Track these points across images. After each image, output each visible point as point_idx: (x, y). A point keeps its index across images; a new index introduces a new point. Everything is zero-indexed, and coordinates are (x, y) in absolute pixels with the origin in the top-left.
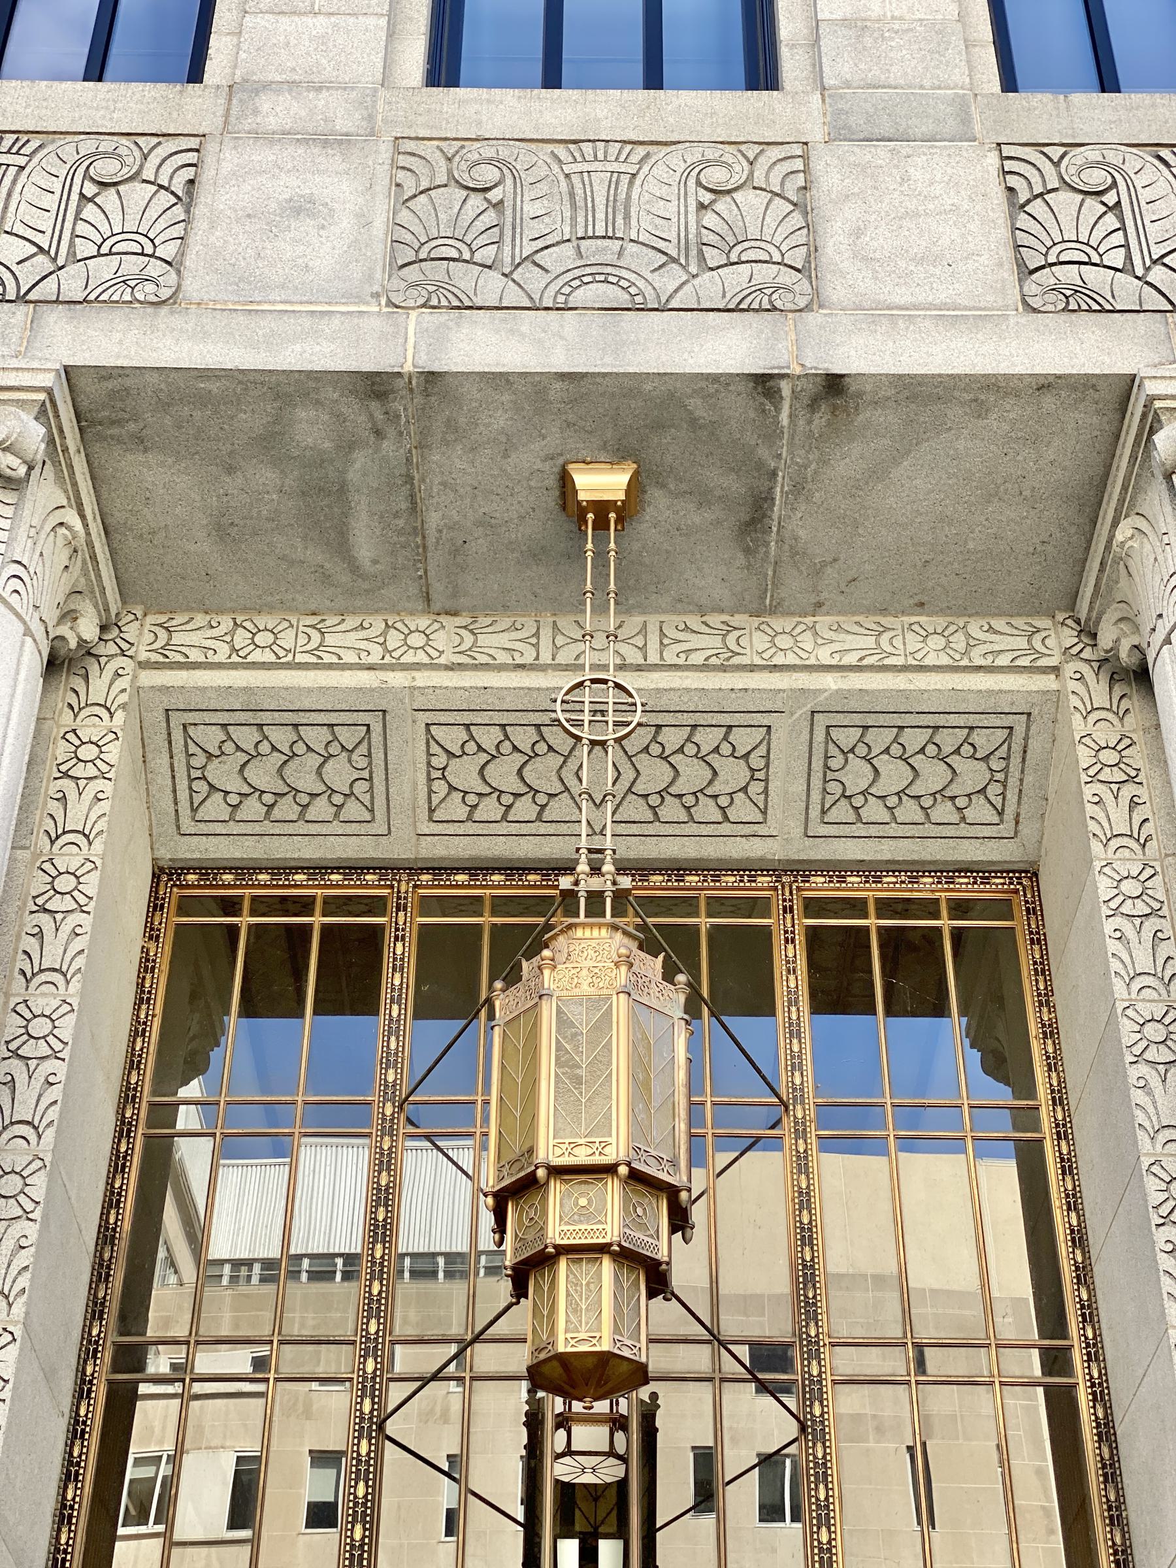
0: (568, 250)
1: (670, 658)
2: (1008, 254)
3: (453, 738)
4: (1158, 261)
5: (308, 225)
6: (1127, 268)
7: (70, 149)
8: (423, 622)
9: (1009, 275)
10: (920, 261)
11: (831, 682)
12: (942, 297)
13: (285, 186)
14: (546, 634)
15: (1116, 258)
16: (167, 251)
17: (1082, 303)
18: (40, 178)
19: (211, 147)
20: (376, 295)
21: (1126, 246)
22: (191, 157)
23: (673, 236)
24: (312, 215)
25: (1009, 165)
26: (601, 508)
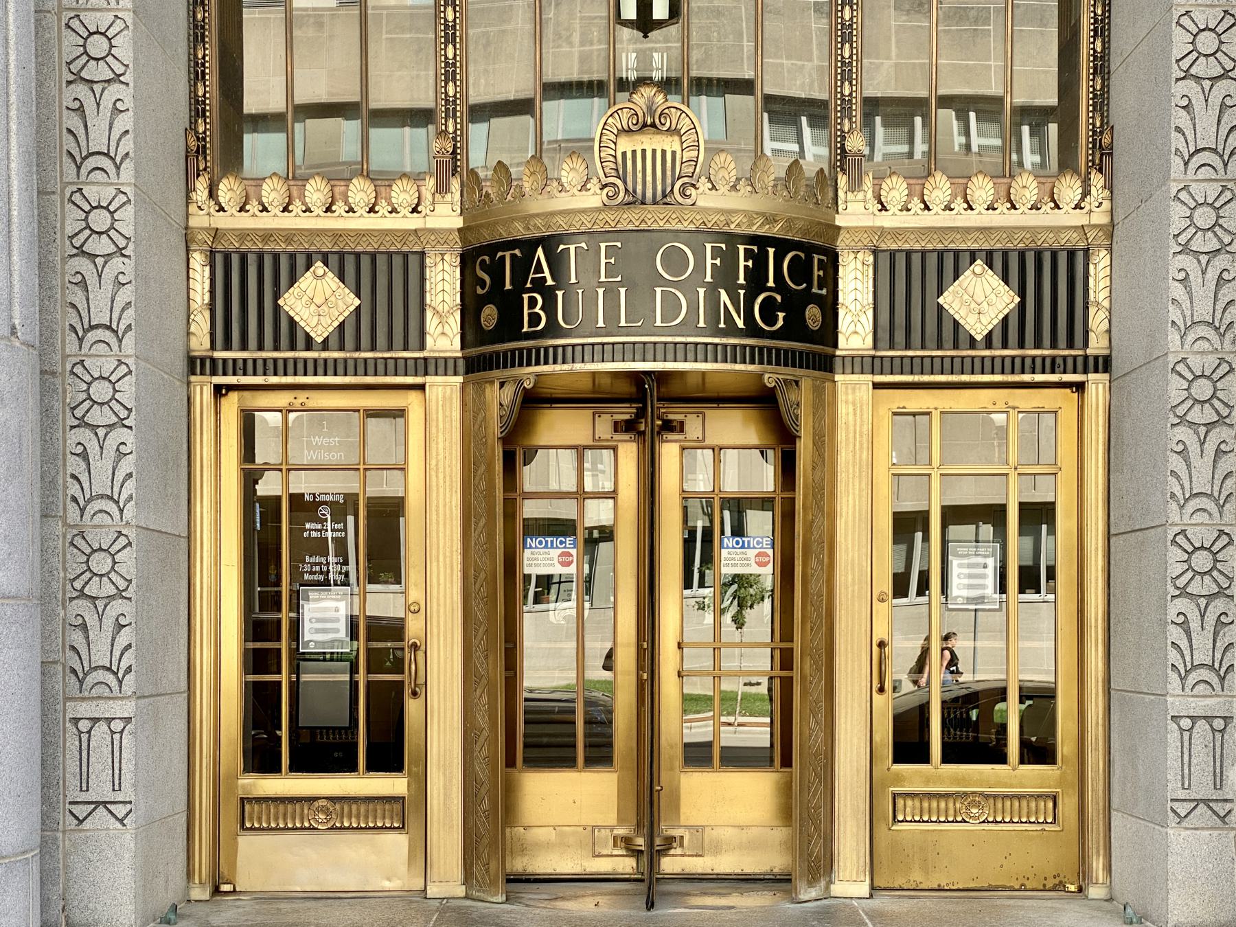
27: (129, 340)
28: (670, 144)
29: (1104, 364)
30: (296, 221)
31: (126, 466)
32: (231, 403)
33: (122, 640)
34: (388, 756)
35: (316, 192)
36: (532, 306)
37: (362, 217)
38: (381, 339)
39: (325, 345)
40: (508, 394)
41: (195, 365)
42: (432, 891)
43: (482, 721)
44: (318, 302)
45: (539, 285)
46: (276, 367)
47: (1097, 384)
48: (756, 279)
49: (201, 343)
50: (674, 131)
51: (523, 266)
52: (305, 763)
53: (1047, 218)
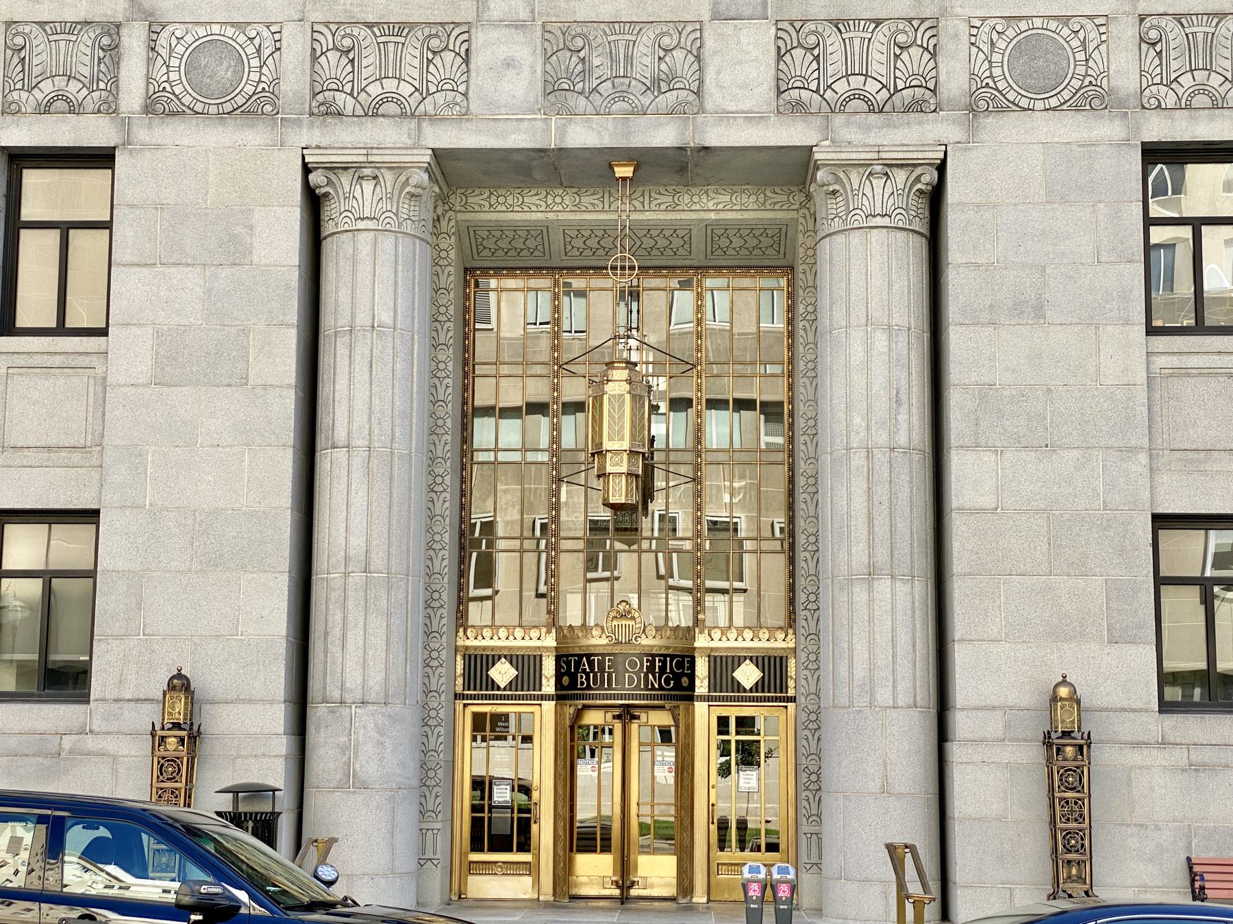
0: (609, 84)
1: (653, 207)
2: (773, 84)
4: (829, 87)
5: (511, 73)
6: (817, 91)
7: (420, 33)
9: (773, 94)
11: (712, 216)
12: (746, 107)
13: (503, 52)
14: (606, 195)
15: (813, 86)
16: (462, 88)
17: (798, 108)
18: (411, 50)
19: (473, 31)
20: (539, 110)
21: (818, 79)
22: (465, 36)
23: (648, 76)
24: (514, 68)
25: (781, 34)
27: (443, 696)
28: (632, 623)
31: (441, 739)
33: (438, 801)
34: (524, 847)
36: (582, 678)
38: (526, 687)
39: (505, 689)
40: (572, 710)
42: (542, 898)
43: (561, 833)
45: (584, 671)
48: (663, 669)
50: (633, 618)
51: (578, 664)
52: (492, 849)
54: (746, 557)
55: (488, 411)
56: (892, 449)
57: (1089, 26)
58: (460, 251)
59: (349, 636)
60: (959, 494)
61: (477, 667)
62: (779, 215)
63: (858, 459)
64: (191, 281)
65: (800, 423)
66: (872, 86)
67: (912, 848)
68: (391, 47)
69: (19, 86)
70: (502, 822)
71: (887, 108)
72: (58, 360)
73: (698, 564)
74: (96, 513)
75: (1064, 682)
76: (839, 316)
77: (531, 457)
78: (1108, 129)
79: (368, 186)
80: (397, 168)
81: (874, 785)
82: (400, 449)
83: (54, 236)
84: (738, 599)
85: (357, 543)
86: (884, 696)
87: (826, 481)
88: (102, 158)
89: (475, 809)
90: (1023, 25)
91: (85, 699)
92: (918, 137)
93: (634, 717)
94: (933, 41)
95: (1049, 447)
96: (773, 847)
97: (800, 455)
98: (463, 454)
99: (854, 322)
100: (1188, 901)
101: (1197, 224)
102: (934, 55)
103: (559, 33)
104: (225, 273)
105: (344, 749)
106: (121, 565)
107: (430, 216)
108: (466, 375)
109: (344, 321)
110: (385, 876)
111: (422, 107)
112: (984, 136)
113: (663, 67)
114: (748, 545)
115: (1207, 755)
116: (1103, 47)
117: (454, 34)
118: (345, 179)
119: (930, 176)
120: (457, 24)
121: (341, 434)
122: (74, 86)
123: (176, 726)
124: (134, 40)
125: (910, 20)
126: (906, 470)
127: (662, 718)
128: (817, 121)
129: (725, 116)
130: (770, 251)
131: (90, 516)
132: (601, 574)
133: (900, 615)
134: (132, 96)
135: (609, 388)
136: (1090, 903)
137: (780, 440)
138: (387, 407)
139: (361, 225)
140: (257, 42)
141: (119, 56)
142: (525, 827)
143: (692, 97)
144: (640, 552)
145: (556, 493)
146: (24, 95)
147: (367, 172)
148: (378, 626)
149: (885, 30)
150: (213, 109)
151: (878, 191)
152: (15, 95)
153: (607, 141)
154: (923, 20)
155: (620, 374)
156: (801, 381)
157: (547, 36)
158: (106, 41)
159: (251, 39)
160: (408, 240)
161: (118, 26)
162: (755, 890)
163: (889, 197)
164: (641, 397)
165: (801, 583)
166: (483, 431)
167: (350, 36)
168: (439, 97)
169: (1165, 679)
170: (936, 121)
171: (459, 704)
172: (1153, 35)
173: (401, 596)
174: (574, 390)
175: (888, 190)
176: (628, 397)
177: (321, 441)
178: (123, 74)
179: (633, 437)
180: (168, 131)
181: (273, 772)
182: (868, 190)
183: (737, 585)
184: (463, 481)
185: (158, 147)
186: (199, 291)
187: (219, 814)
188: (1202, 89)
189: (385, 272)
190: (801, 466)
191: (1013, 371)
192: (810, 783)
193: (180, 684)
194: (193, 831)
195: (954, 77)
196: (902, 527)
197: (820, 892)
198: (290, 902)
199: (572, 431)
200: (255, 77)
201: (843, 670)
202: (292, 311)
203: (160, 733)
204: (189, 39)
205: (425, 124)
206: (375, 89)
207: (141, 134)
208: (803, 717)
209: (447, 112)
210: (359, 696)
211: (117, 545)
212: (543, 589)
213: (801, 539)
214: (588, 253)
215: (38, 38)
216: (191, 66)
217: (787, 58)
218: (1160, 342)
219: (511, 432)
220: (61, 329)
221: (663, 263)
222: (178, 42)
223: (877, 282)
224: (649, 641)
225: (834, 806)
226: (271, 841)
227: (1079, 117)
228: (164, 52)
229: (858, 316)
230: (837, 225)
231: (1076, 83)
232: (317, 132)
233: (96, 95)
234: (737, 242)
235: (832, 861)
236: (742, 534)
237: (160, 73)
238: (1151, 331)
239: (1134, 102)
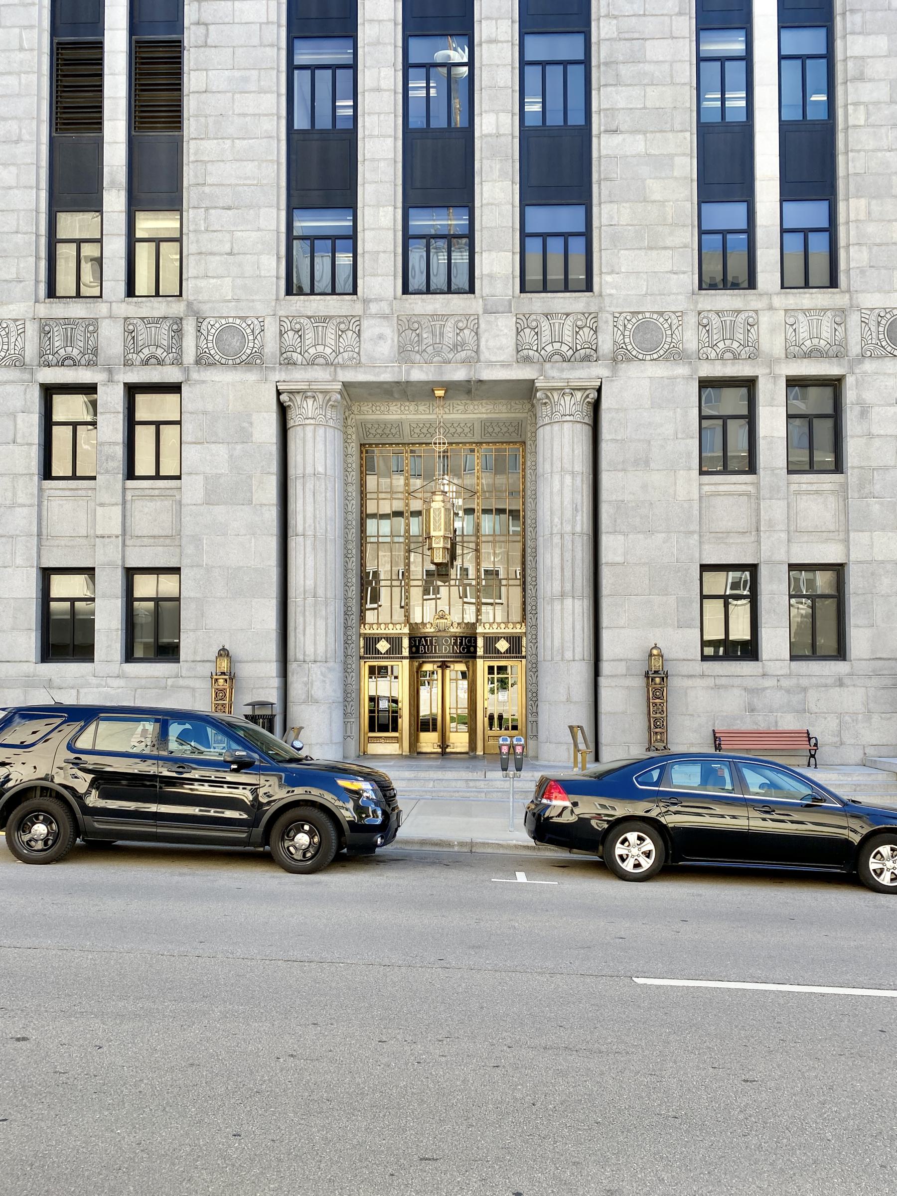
0: (431, 347)
2: (514, 347)
3: (415, 426)
5: (382, 342)
6: (537, 351)
8: (407, 404)
9: (515, 353)
10: (498, 349)
12: (502, 359)
13: (377, 331)
16: (357, 350)
17: (527, 360)
18: (330, 330)
22: (358, 323)
26: (440, 397)
29: (524, 657)
30: (379, 631)
32: (367, 664)
34: (395, 729)
35: (383, 626)
36: (421, 648)
37: (391, 631)
41: (361, 658)
44: (383, 646)
46: (375, 658)
47: (524, 660)
48: (461, 643)
49: (362, 654)
51: (420, 641)
52: (379, 731)
53: (514, 631)
54: (503, 588)
55: (373, 516)
56: (573, 534)
57: (673, 317)
58: (358, 434)
59: (307, 629)
60: (606, 556)
61: (371, 642)
62: (518, 415)
63: (557, 540)
64: (221, 451)
65: (528, 521)
66: (565, 348)
67: (581, 727)
68: (320, 328)
69: (132, 351)
70: (384, 718)
71: (572, 359)
72: (156, 492)
73: (478, 591)
74: (179, 569)
75: (656, 647)
76: (547, 467)
77: (396, 539)
78: (682, 370)
79: (310, 402)
80: (325, 392)
81: (564, 698)
82: (330, 536)
83: (153, 428)
84: (498, 607)
85: (310, 583)
86: (568, 655)
87: (540, 550)
88: (175, 388)
89: (371, 711)
90: (640, 316)
91: (177, 660)
92: (587, 374)
93: (447, 667)
94: (595, 325)
95: (651, 532)
96: (515, 728)
97: (528, 537)
98: (362, 538)
99: (555, 470)
100: (712, 751)
101: (725, 419)
102: (596, 332)
103: (405, 321)
104: (239, 447)
105: (306, 684)
106: (192, 595)
107: (342, 417)
108: (362, 499)
109: (300, 471)
110: (327, 744)
111: (336, 360)
112: (620, 373)
113: (459, 338)
114: (504, 582)
115: (723, 681)
116: (680, 328)
117: (352, 321)
118: (298, 398)
119: (593, 395)
120: (354, 316)
121: (300, 529)
122: (160, 351)
123: (223, 673)
124: (189, 327)
125: (583, 314)
126: (580, 544)
127: (462, 667)
128: (537, 366)
129: (491, 364)
130: (514, 434)
131: (176, 570)
132: (432, 596)
133: (576, 615)
134: (189, 356)
135: (433, 504)
136: (666, 752)
137: (518, 529)
138: (323, 515)
139: (307, 422)
140: (252, 326)
141: (182, 335)
142: (395, 720)
143: (473, 354)
144: (450, 586)
145: (408, 558)
146: (135, 356)
147: (309, 394)
148: (321, 624)
149: (571, 319)
150: (230, 362)
151: (568, 403)
152: (130, 356)
153: (431, 378)
154: (590, 314)
155: (438, 498)
156: (529, 500)
157: (400, 322)
158: (175, 327)
159: (249, 325)
160: (332, 430)
161: (181, 319)
162: (505, 750)
163: (573, 407)
164: (449, 509)
165: (528, 600)
166: (371, 525)
167: (299, 323)
168: (346, 355)
169: (704, 644)
170: (596, 366)
171: (362, 662)
172: (705, 321)
173: (332, 608)
174: (416, 505)
175: (572, 402)
176: (443, 510)
177: (290, 532)
178: (184, 344)
179: (446, 530)
180: (208, 373)
181: (273, 696)
182: (562, 402)
183: (498, 601)
184: (362, 552)
185: (203, 382)
186: (226, 456)
187: (246, 717)
188: (728, 350)
189: (320, 446)
190: (529, 543)
191: (634, 494)
192: (533, 698)
193: (224, 653)
194: (231, 725)
195: (606, 345)
196: (578, 573)
197: (537, 748)
198: (280, 759)
199: (415, 526)
200: (251, 345)
201: (549, 643)
202: (274, 466)
203: (215, 677)
204: (217, 325)
205: (339, 369)
206: (312, 351)
207: (195, 376)
208: (530, 666)
209: (349, 363)
210: (312, 659)
211: (189, 587)
212: (403, 604)
213: (528, 579)
214: (422, 435)
215: (141, 326)
216: (218, 339)
217: (522, 333)
218: (706, 479)
219: (385, 526)
220: (158, 477)
221: (460, 441)
222: (212, 326)
223: (567, 449)
224: (454, 630)
225: (543, 708)
226: (271, 730)
227: (668, 363)
228: (205, 333)
229: (557, 465)
230: (547, 420)
231: (666, 346)
232: (283, 374)
233: (171, 355)
234: (497, 430)
235: (542, 735)
236: (501, 577)
237: (203, 344)
238: (702, 473)
239: (695, 356)
